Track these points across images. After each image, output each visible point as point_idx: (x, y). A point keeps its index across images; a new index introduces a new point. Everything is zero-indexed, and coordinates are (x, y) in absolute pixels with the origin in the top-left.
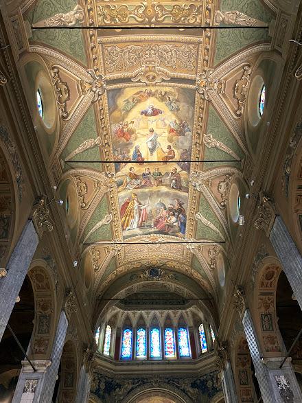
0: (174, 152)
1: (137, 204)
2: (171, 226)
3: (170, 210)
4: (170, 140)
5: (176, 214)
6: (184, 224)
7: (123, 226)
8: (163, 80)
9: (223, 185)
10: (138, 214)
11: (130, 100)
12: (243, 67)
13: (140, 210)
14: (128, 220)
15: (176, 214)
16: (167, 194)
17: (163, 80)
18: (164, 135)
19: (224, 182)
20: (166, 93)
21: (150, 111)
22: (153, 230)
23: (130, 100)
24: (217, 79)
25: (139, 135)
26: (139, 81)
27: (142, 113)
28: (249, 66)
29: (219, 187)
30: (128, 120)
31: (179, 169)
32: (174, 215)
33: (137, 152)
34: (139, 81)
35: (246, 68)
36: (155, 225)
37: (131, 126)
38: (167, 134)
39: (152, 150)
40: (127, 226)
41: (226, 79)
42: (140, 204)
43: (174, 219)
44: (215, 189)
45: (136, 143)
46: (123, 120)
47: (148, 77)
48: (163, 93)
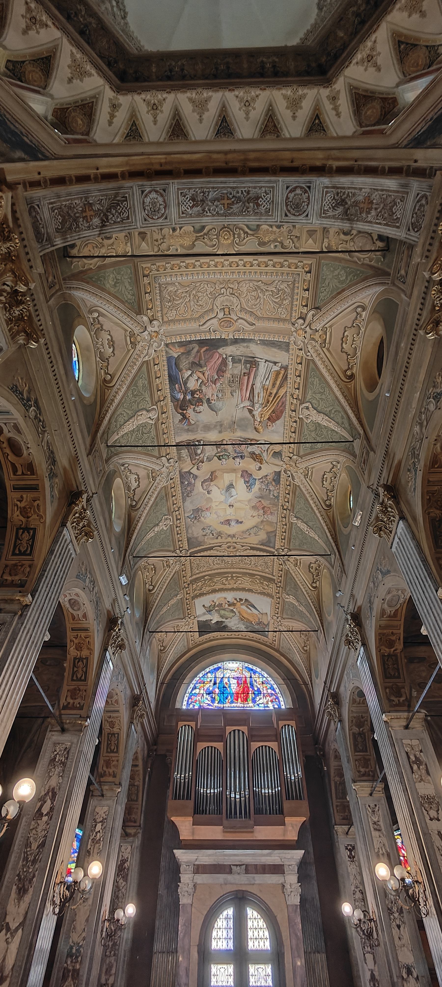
0: (203, 488)
1: (256, 413)
2: (196, 365)
3: (200, 401)
4: (209, 500)
5: (189, 397)
6: (173, 380)
7: (285, 378)
8: (220, 546)
9: (134, 485)
10: (256, 393)
11: (252, 534)
12: (154, 587)
13: (251, 399)
14: (274, 385)
15: (189, 397)
16: (207, 428)
17: (220, 546)
18: (217, 504)
19: (134, 490)
20: (217, 538)
21: (233, 523)
22: (229, 350)
23: (252, 534)
24: (172, 567)
25: (247, 503)
26: (243, 546)
27: (241, 522)
28: (150, 590)
29: (138, 479)
30: (257, 520)
31: (194, 471)
32: (193, 393)
33: (249, 486)
34: (243, 546)
35: (151, 588)
36: (224, 362)
37: (255, 514)
38: (213, 505)
39: (231, 486)
40: (278, 373)
41: (165, 570)
42: (250, 411)
43: (192, 385)
44: (142, 473)
45: (250, 496)
46: (262, 521)
47: (235, 548)
48: (219, 537)
